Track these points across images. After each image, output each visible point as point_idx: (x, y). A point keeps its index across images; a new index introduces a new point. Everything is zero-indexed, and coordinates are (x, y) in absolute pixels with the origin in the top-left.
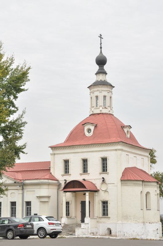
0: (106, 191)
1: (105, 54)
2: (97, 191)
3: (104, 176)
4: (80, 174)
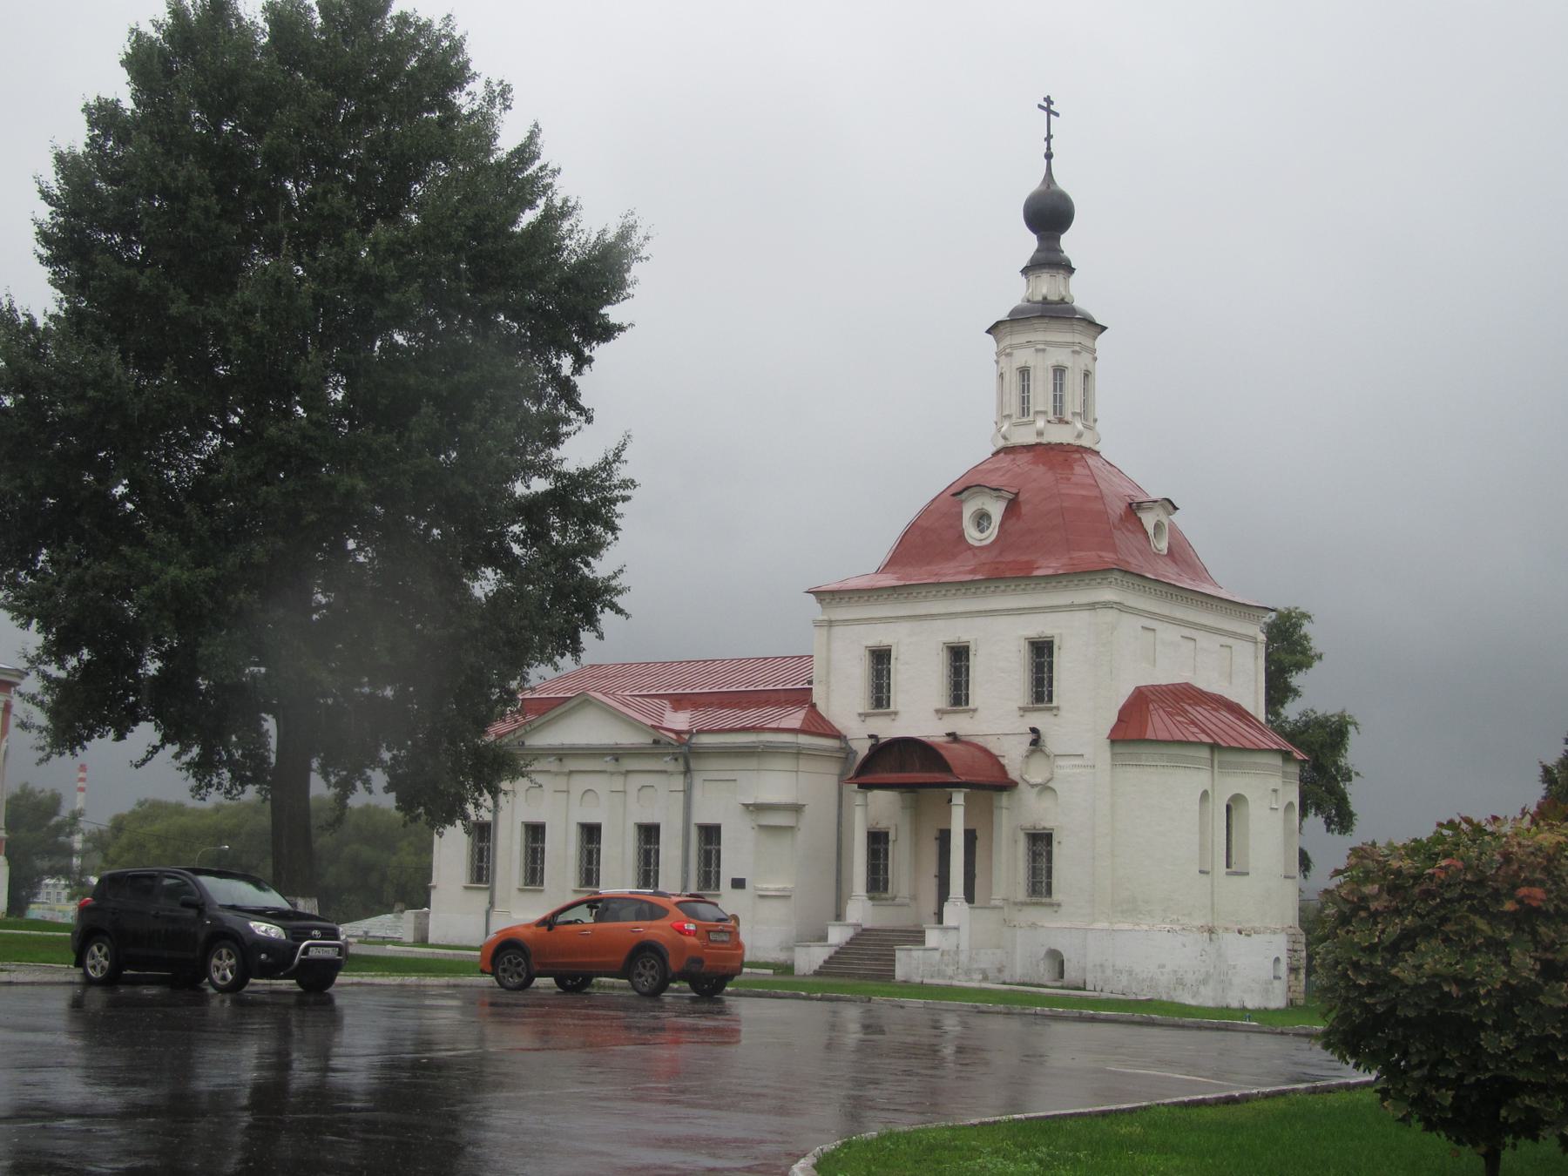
0: (1045, 788)
1: (1063, 183)
3: (1038, 720)
4: (937, 711)
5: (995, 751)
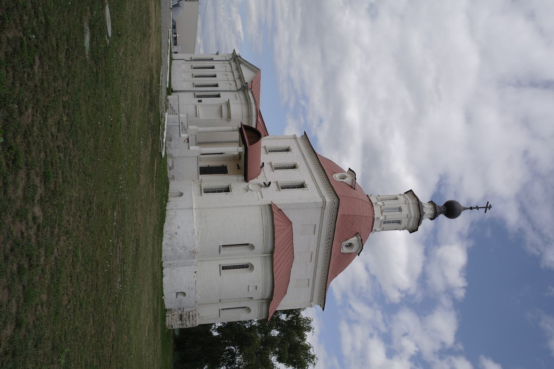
2: (246, 180)
5: (259, 177)
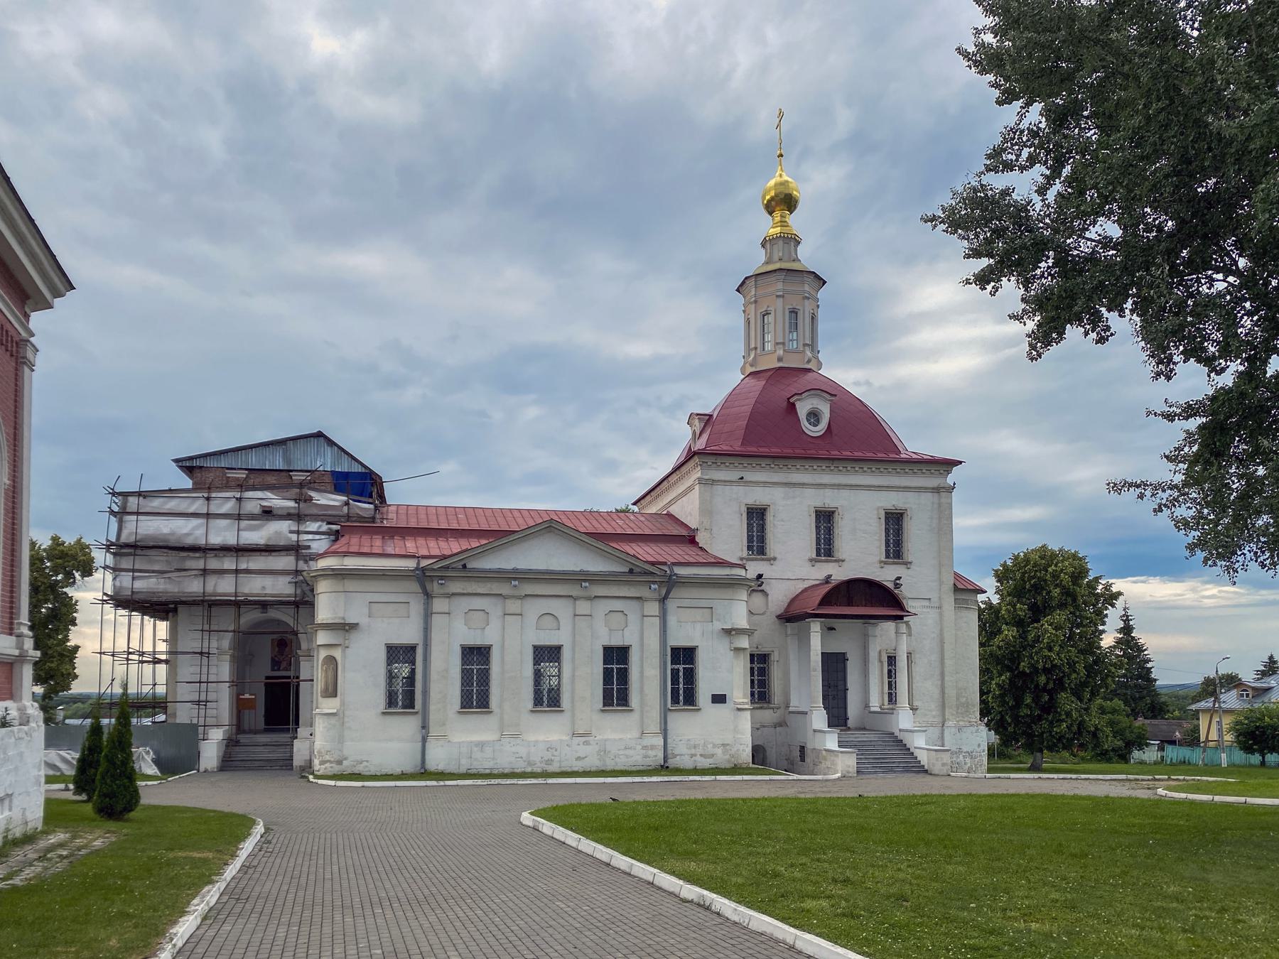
4: (811, 560)
